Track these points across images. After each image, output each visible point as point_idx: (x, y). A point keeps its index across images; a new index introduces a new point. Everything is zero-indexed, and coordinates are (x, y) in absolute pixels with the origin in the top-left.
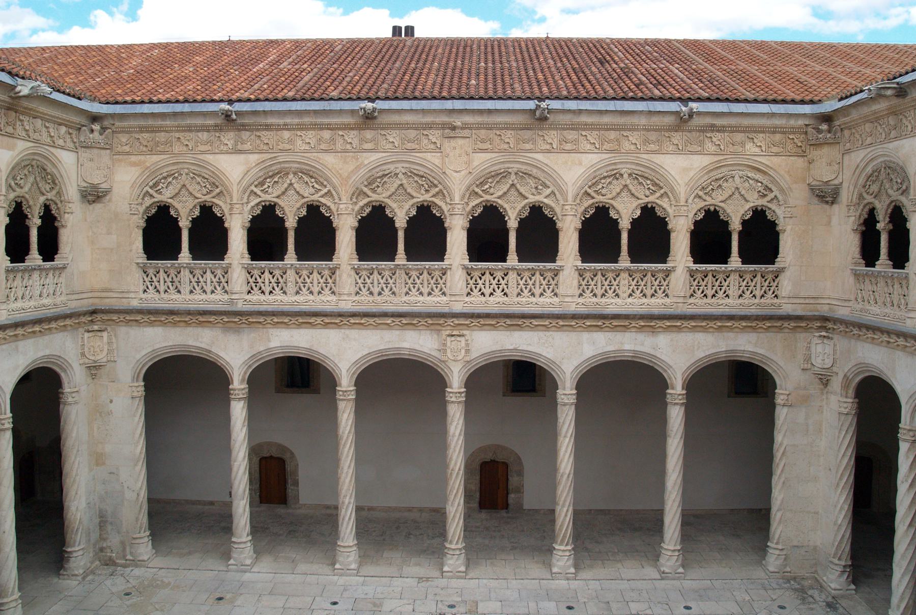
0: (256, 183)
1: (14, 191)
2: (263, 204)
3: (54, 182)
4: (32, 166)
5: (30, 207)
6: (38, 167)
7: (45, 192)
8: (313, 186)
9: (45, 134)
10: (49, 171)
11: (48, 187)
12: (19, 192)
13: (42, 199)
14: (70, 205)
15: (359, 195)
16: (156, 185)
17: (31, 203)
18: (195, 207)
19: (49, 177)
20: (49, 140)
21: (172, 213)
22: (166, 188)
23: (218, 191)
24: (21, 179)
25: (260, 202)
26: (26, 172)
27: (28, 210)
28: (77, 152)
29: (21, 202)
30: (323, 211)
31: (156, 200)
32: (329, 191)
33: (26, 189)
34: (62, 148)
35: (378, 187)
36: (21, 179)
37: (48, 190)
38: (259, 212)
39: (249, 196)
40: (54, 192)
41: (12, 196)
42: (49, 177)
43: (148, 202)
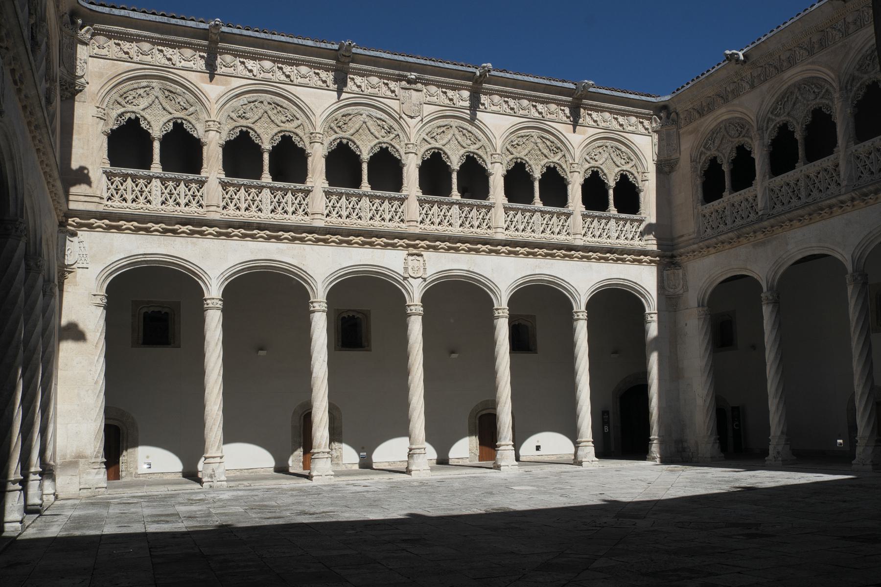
0: (771, 109)
1: (589, 163)
2: (778, 125)
3: (629, 158)
4: (606, 147)
5: (605, 174)
6: (612, 147)
7: (619, 164)
8: (814, 92)
9: (614, 123)
10: (623, 150)
11: (623, 162)
12: (593, 163)
13: (617, 169)
14: (646, 174)
15: (853, 80)
16: (706, 144)
17: (606, 171)
18: (731, 150)
19: (624, 154)
20: (618, 127)
21: (719, 162)
22: (714, 142)
23: (746, 129)
24: (595, 155)
25: (775, 125)
26: (600, 150)
27: (604, 177)
28: (651, 136)
29: (597, 172)
30: (824, 110)
31: (707, 155)
32: (827, 90)
33: (601, 162)
34: (633, 133)
35: (868, 65)
36: (595, 155)
37: (623, 163)
38: (775, 134)
39: (768, 123)
40: (630, 165)
41: (587, 166)
42: (624, 154)
43: (703, 158)
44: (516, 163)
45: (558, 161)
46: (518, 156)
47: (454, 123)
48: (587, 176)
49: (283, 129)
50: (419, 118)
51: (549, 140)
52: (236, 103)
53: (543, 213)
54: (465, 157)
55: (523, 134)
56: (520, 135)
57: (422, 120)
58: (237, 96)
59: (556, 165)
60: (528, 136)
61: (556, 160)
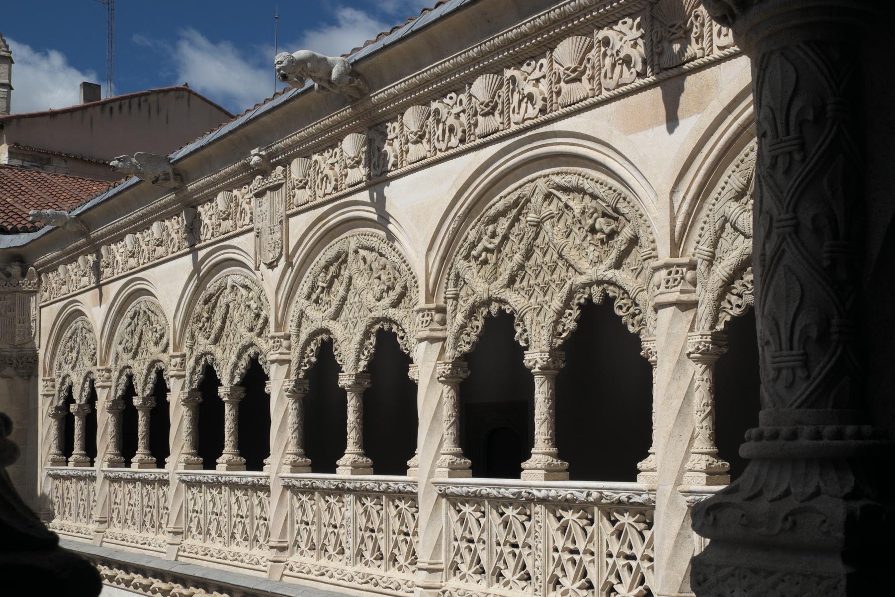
44: (488, 318)
45: (610, 274)
46: (485, 297)
47: (350, 240)
48: (733, 309)
49: (155, 358)
50: (282, 263)
51: (581, 191)
52: (121, 327)
53: (554, 505)
54: (373, 339)
55: (500, 206)
56: (492, 212)
57: (289, 264)
58: (121, 312)
59: (611, 291)
60: (516, 203)
61: (603, 271)
